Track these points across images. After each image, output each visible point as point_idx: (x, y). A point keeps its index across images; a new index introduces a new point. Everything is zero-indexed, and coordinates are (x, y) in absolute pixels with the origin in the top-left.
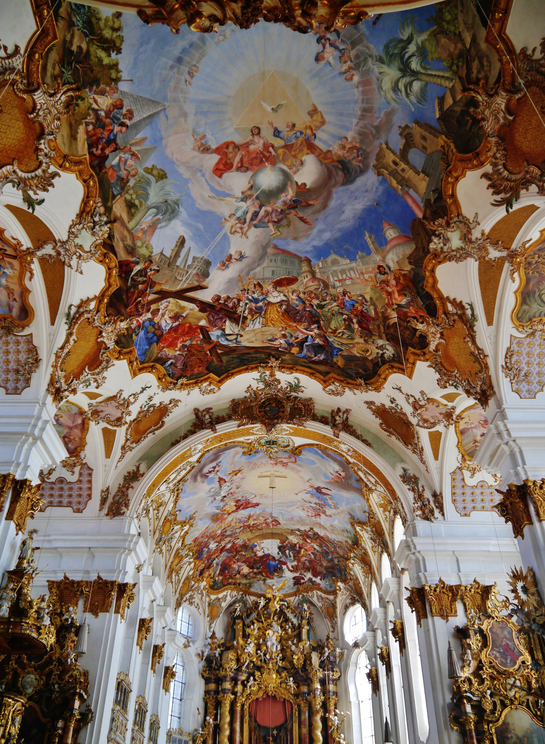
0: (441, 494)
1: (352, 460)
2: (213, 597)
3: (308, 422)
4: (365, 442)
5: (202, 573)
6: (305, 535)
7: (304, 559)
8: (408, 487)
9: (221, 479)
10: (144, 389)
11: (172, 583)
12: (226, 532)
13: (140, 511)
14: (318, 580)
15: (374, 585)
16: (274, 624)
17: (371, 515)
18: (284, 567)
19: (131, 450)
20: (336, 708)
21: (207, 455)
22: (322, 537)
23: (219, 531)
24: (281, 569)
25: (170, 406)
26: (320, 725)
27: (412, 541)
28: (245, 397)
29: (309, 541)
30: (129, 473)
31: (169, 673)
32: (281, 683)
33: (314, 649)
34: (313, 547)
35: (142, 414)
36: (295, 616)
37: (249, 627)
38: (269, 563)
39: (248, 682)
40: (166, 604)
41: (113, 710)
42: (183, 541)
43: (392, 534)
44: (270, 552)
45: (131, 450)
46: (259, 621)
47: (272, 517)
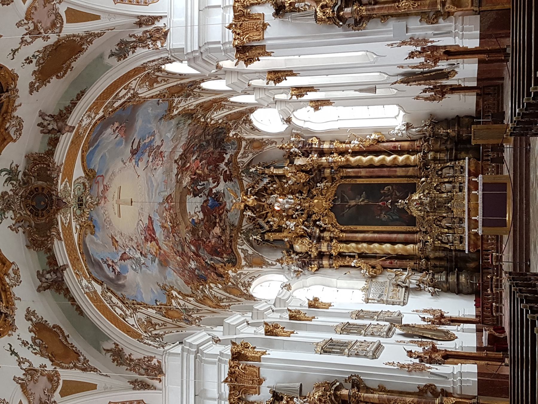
0: (138, 17)
1: (101, 114)
2: (243, 263)
3: (56, 161)
4: (79, 97)
5: (220, 276)
6: (182, 169)
7: (206, 170)
8: (131, 53)
9: (122, 258)
10: (13, 352)
11: (230, 305)
12: (178, 251)
13: (156, 344)
14: (227, 157)
15: (232, 99)
16: (269, 202)
17: (161, 95)
18: (214, 191)
19: (88, 361)
20: (344, 143)
21: (94, 274)
22: (185, 151)
23: (178, 258)
24: (216, 194)
25: (34, 319)
26: (358, 157)
27: (188, 54)
28: (24, 233)
29: (189, 165)
30: (114, 360)
31: (314, 304)
32: (322, 195)
33: (292, 162)
34: (194, 161)
35: (44, 352)
36: (261, 180)
37: (271, 226)
38: (210, 206)
39: (321, 226)
40: (251, 309)
41: (349, 356)
42: (188, 296)
43: (181, 76)
44: (199, 206)
45: (88, 361)
46: (266, 217)
47: (163, 203)
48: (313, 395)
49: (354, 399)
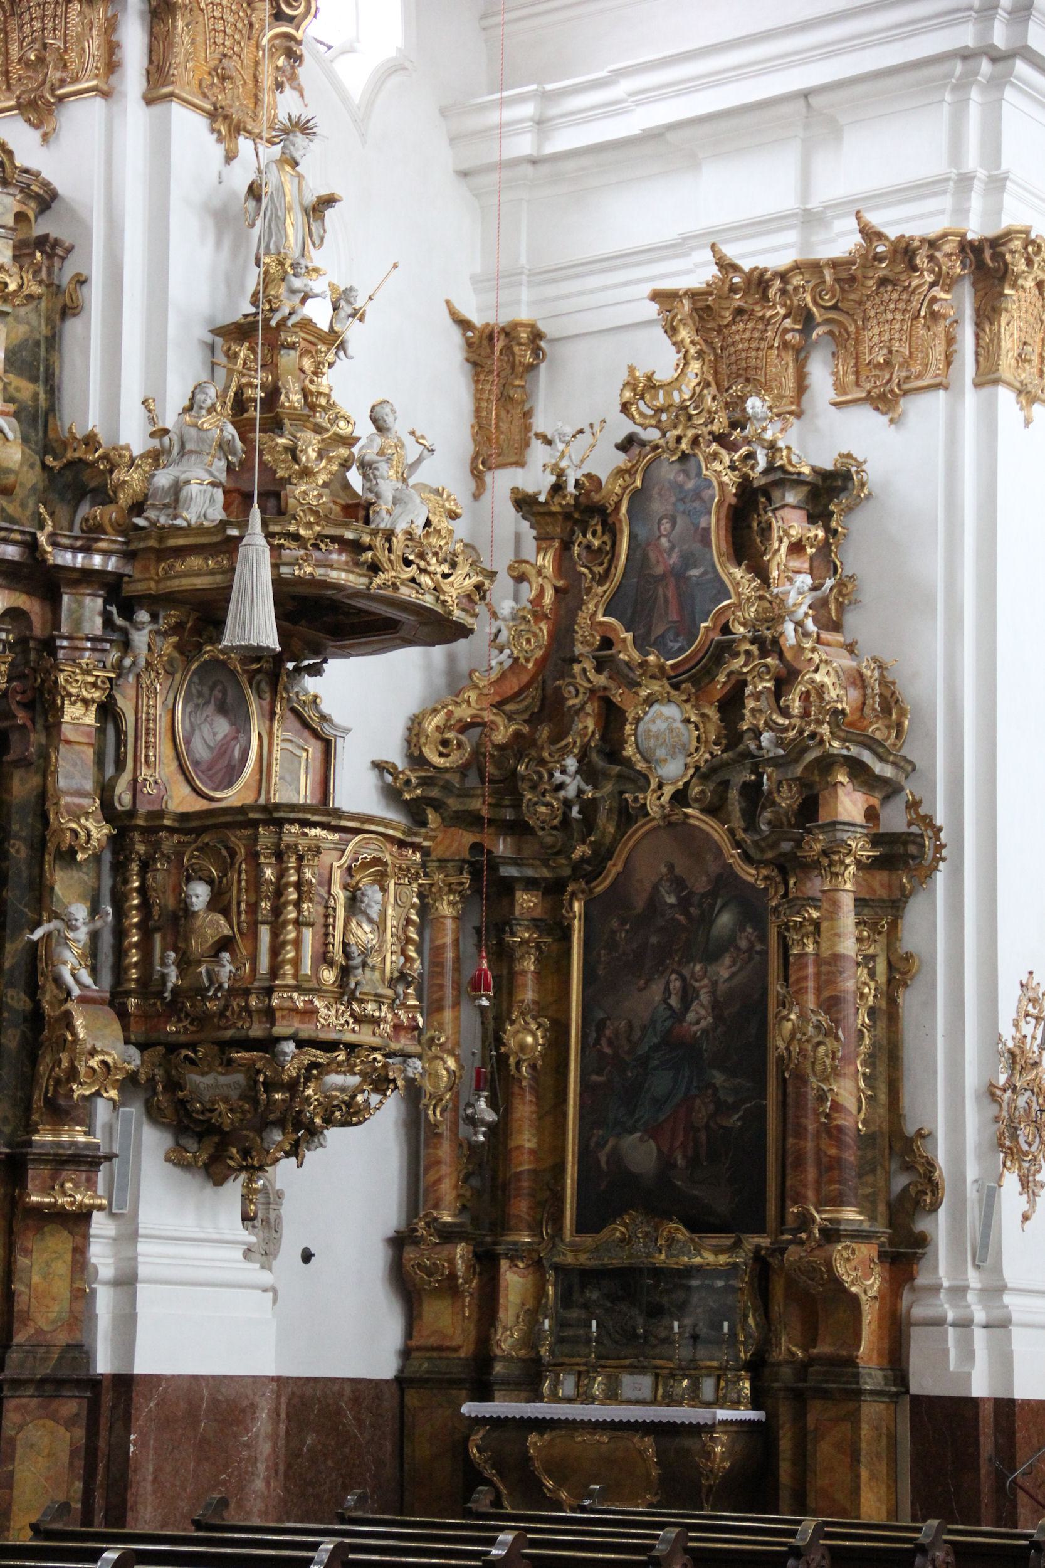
48: (826, 662)
49: (818, 847)
